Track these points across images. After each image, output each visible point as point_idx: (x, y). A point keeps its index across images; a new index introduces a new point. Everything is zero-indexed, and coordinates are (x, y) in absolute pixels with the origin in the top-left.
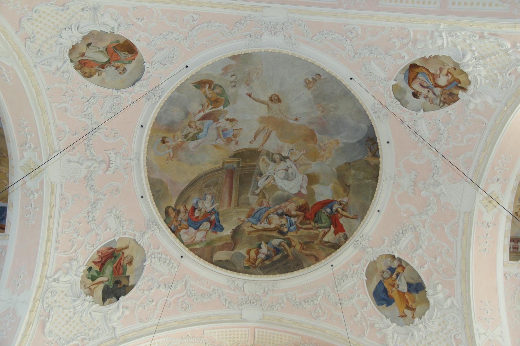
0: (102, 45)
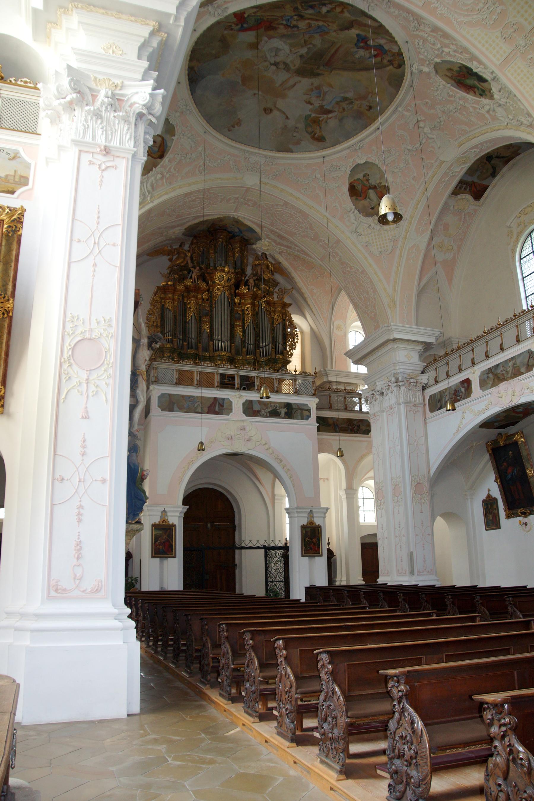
0: (365, 202)
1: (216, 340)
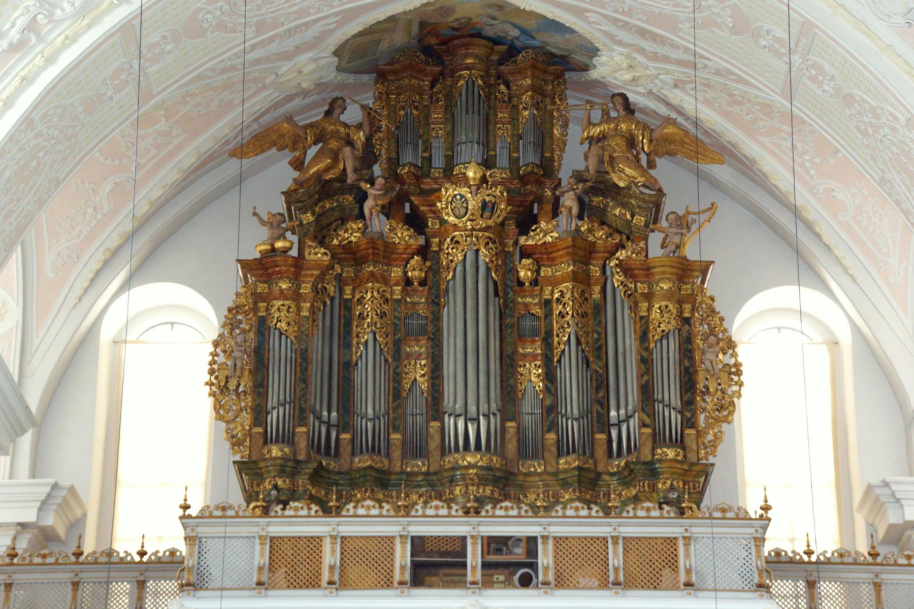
1: (450, 415)
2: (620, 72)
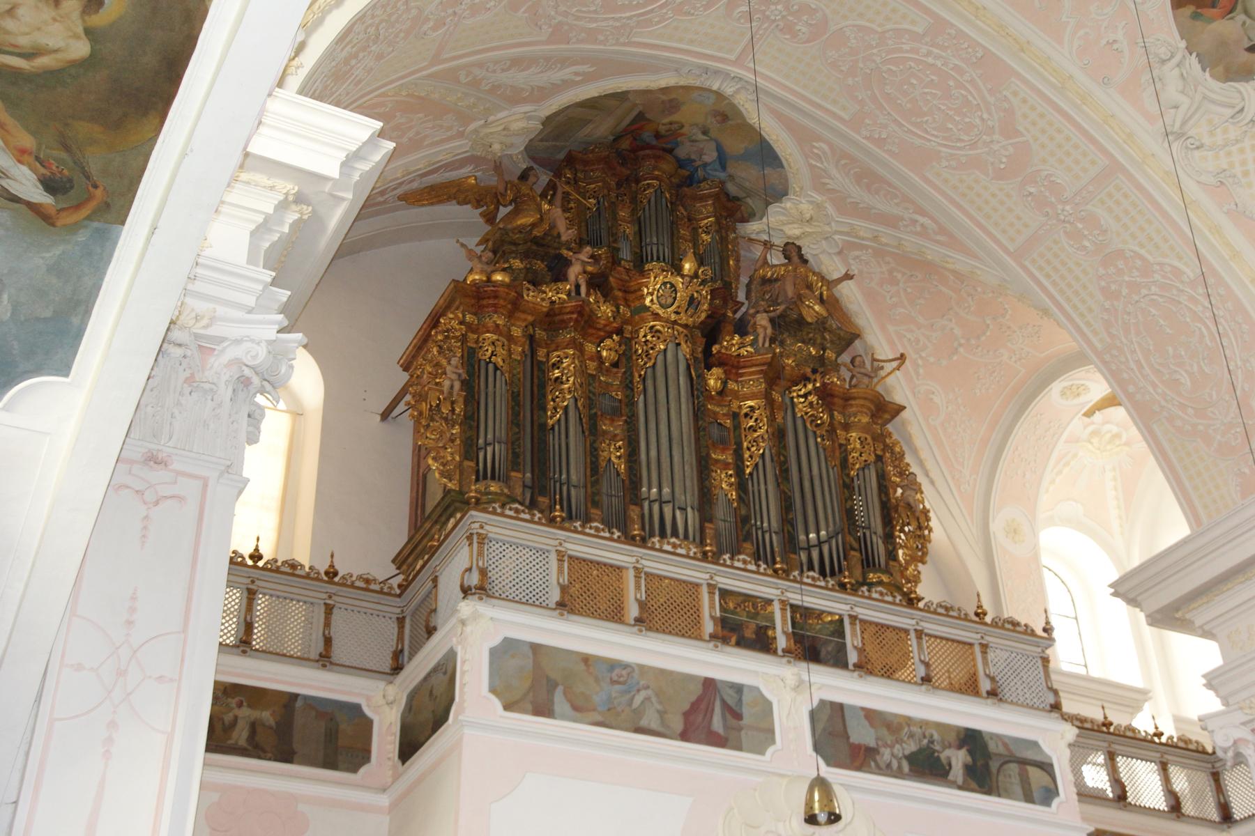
2: (791, 226)
